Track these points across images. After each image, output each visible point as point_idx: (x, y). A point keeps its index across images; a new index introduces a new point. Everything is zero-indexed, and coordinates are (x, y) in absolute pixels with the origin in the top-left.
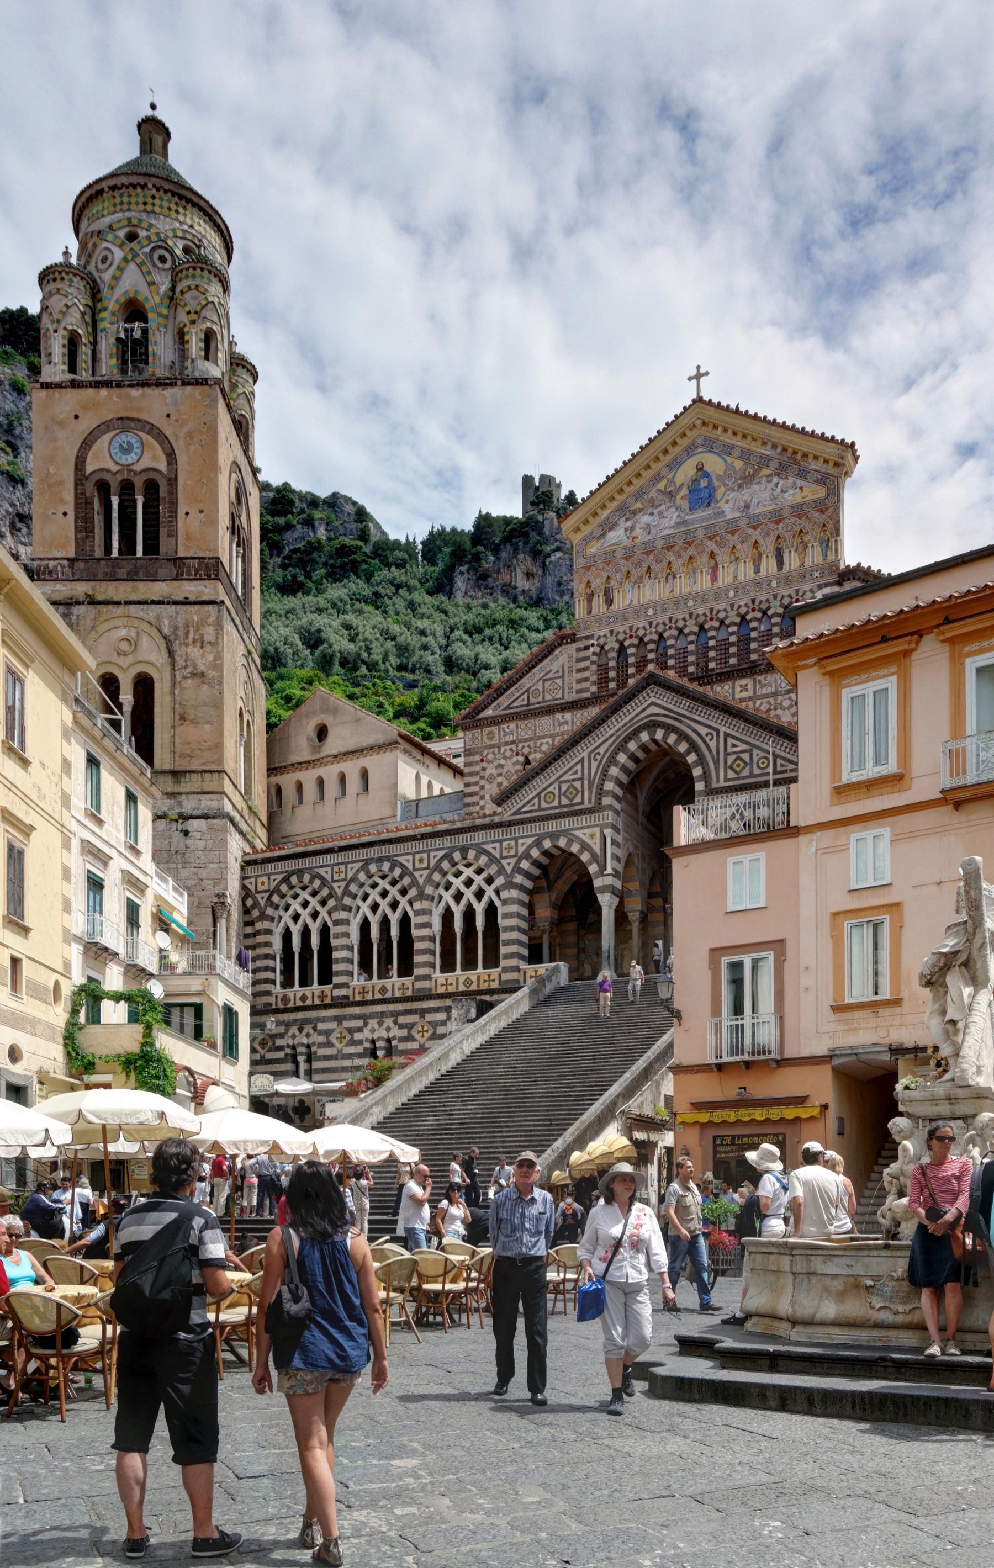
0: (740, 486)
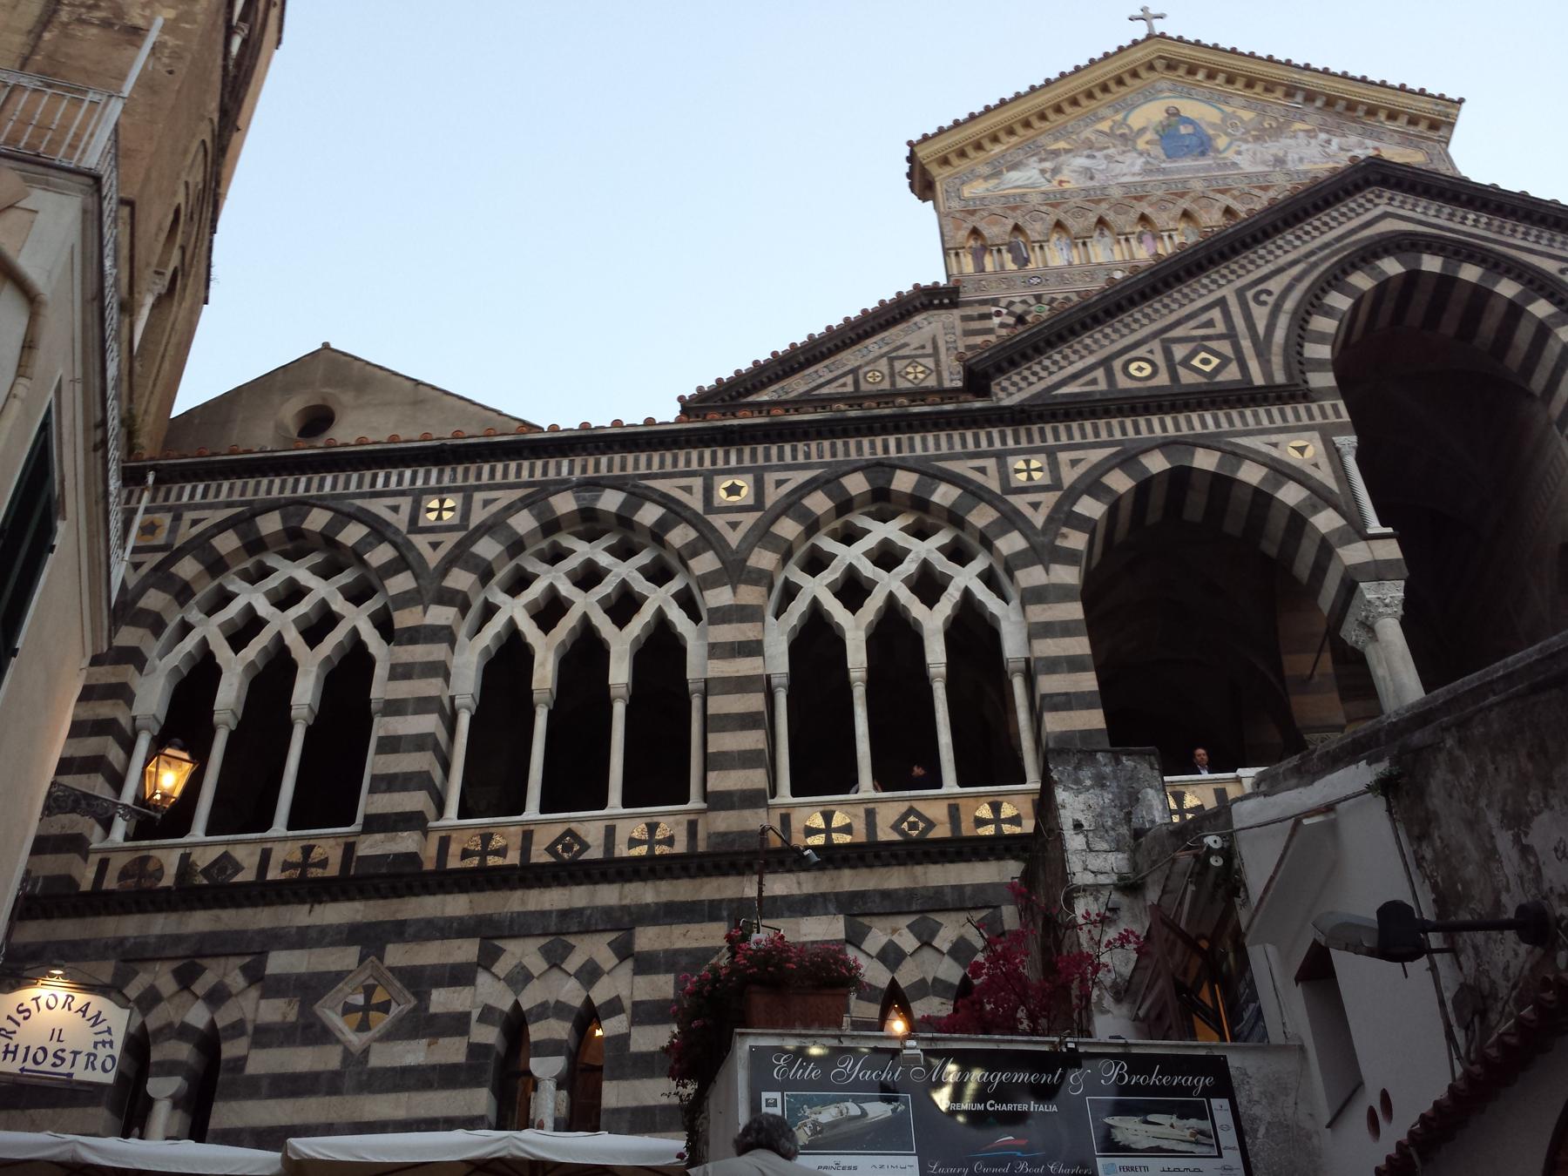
0: (1257, 139)
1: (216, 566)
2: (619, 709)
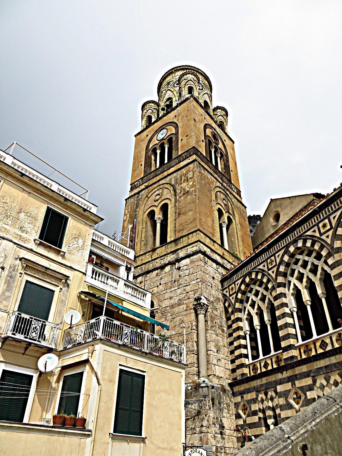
1: (244, 293)
2: (324, 300)
